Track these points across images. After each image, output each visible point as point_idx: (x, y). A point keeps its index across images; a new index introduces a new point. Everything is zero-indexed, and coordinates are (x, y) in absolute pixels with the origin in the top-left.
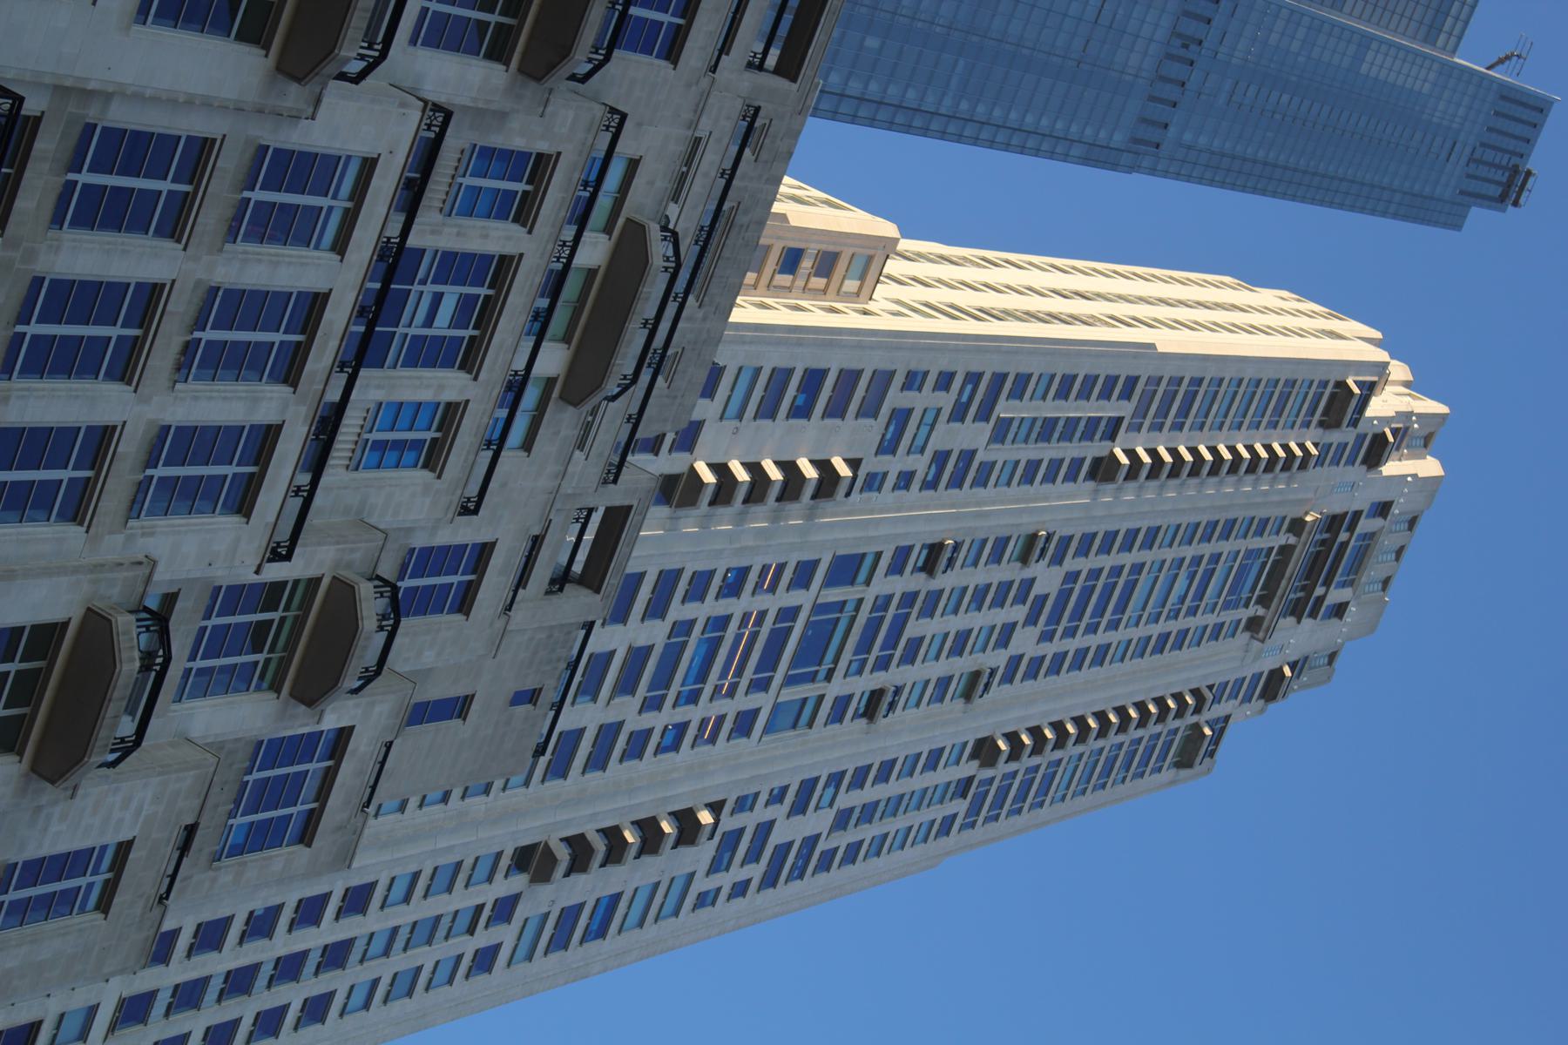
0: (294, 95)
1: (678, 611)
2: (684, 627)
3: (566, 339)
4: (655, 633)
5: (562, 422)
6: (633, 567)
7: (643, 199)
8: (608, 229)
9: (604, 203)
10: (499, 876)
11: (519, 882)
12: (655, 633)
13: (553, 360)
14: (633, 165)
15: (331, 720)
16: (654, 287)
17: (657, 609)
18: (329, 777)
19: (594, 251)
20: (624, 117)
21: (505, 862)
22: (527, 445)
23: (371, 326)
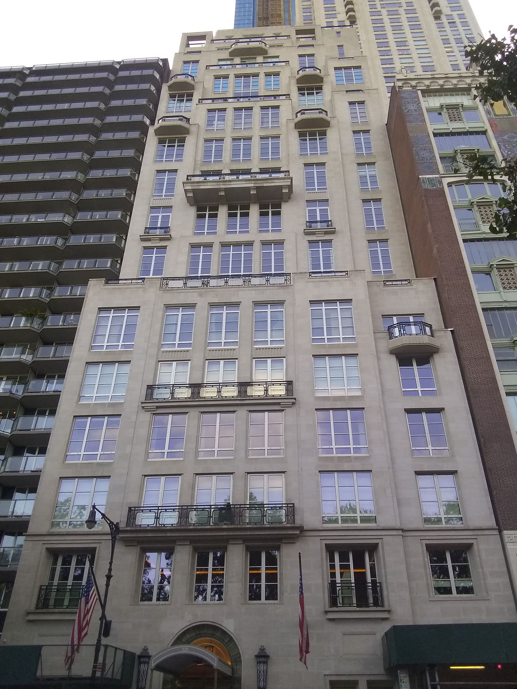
0: (193, 129)
1: (379, 9)
2: (383, 6)
3: (255, 58)
4: (384, 12)
5: (272, 52)
6: (303, 25)
7: (225, 55)
8: (232, 59)
9: (228, 62)
10: (441, 22)
11: (443, 17)
12: (384, 12)
13: (260, 59)
14: (220, 60)
15: (332, 72)
16: (240, 45)
17: (379, 13)
18: (346, 68)
19: (237, 60)
20: (207, 66)
21: (438, 22)
22: (278, 57)
23: (241, 97)
